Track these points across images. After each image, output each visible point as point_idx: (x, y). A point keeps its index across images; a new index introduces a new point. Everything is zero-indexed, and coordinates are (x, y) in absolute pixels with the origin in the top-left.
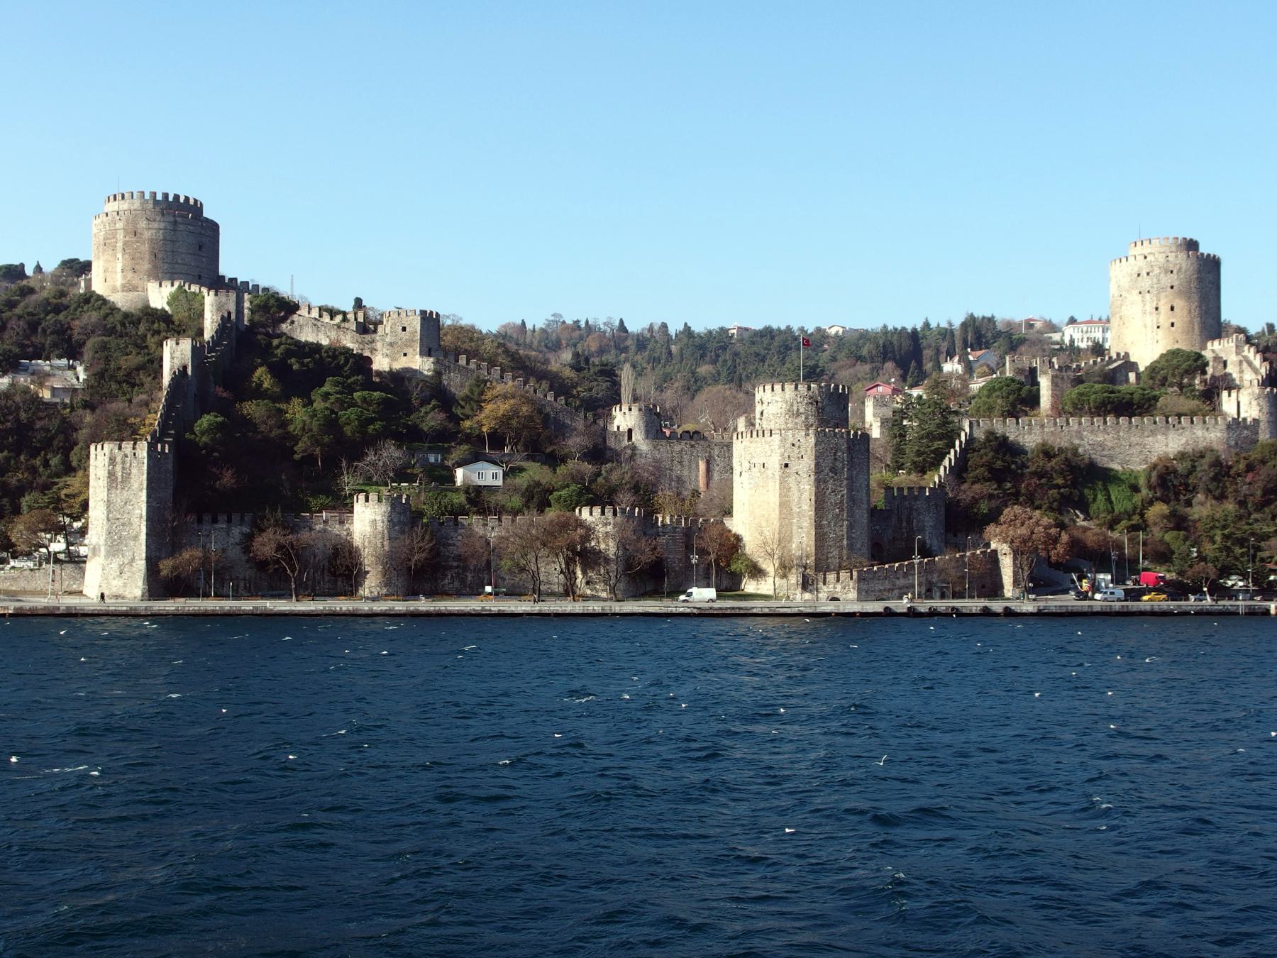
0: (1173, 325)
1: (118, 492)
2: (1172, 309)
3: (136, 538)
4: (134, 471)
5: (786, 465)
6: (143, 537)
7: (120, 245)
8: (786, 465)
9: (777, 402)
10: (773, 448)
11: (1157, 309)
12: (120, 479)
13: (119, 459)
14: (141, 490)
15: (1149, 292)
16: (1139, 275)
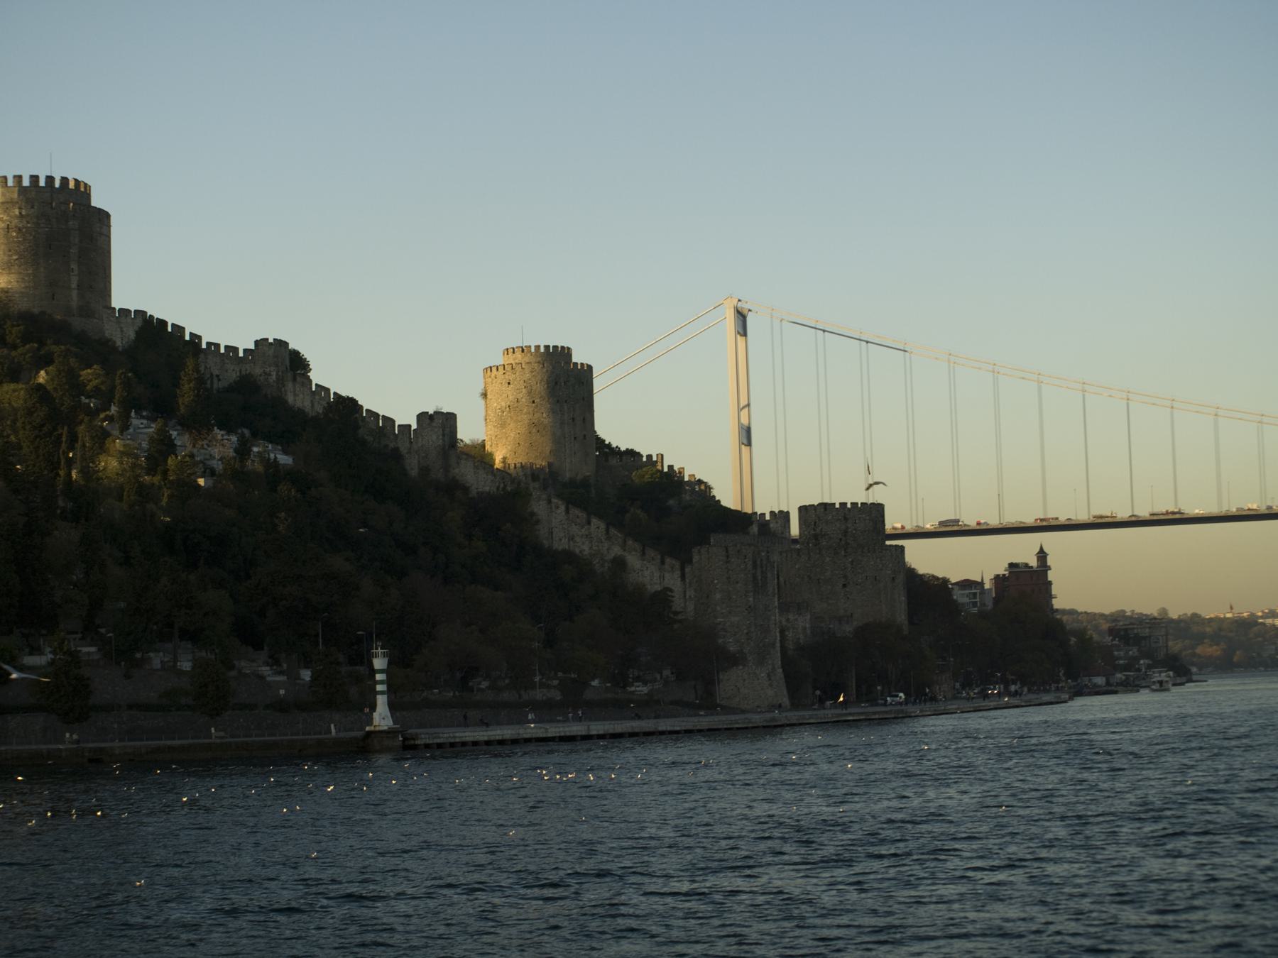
0: (585, 436)
1: (760, 597)
2: (584, 419)
3: (773, 644)
4: (769, 575)
5: (893, 578)
6: (778, 645)
7: (74, 250)
8: (893, 578)
9: (865, 520)
10: (884, 562)
11: (573, 419)
12: (760, 585)
13: (758, 563)
14: (774, 596)
15: (566, 401)
16: (556, 383)
